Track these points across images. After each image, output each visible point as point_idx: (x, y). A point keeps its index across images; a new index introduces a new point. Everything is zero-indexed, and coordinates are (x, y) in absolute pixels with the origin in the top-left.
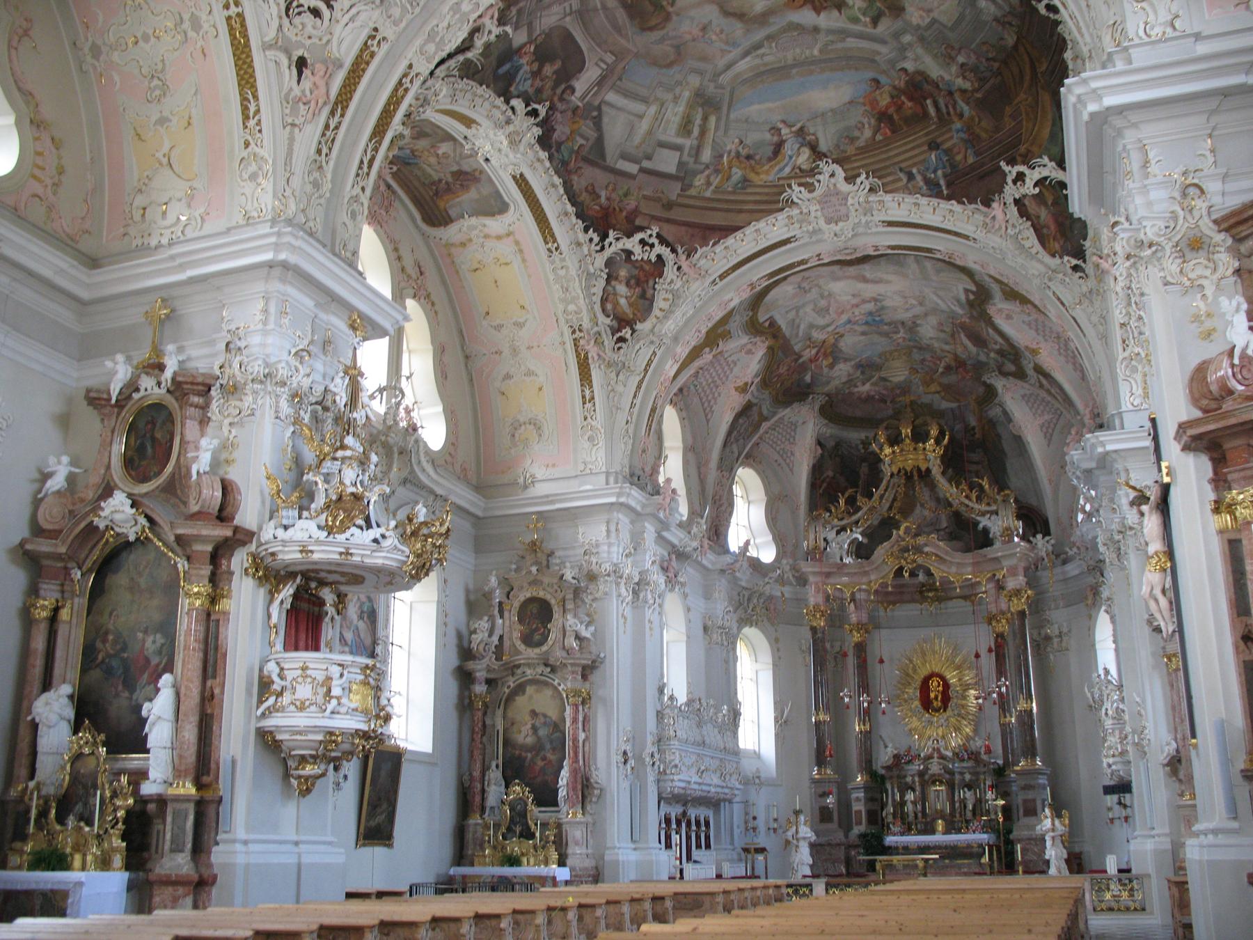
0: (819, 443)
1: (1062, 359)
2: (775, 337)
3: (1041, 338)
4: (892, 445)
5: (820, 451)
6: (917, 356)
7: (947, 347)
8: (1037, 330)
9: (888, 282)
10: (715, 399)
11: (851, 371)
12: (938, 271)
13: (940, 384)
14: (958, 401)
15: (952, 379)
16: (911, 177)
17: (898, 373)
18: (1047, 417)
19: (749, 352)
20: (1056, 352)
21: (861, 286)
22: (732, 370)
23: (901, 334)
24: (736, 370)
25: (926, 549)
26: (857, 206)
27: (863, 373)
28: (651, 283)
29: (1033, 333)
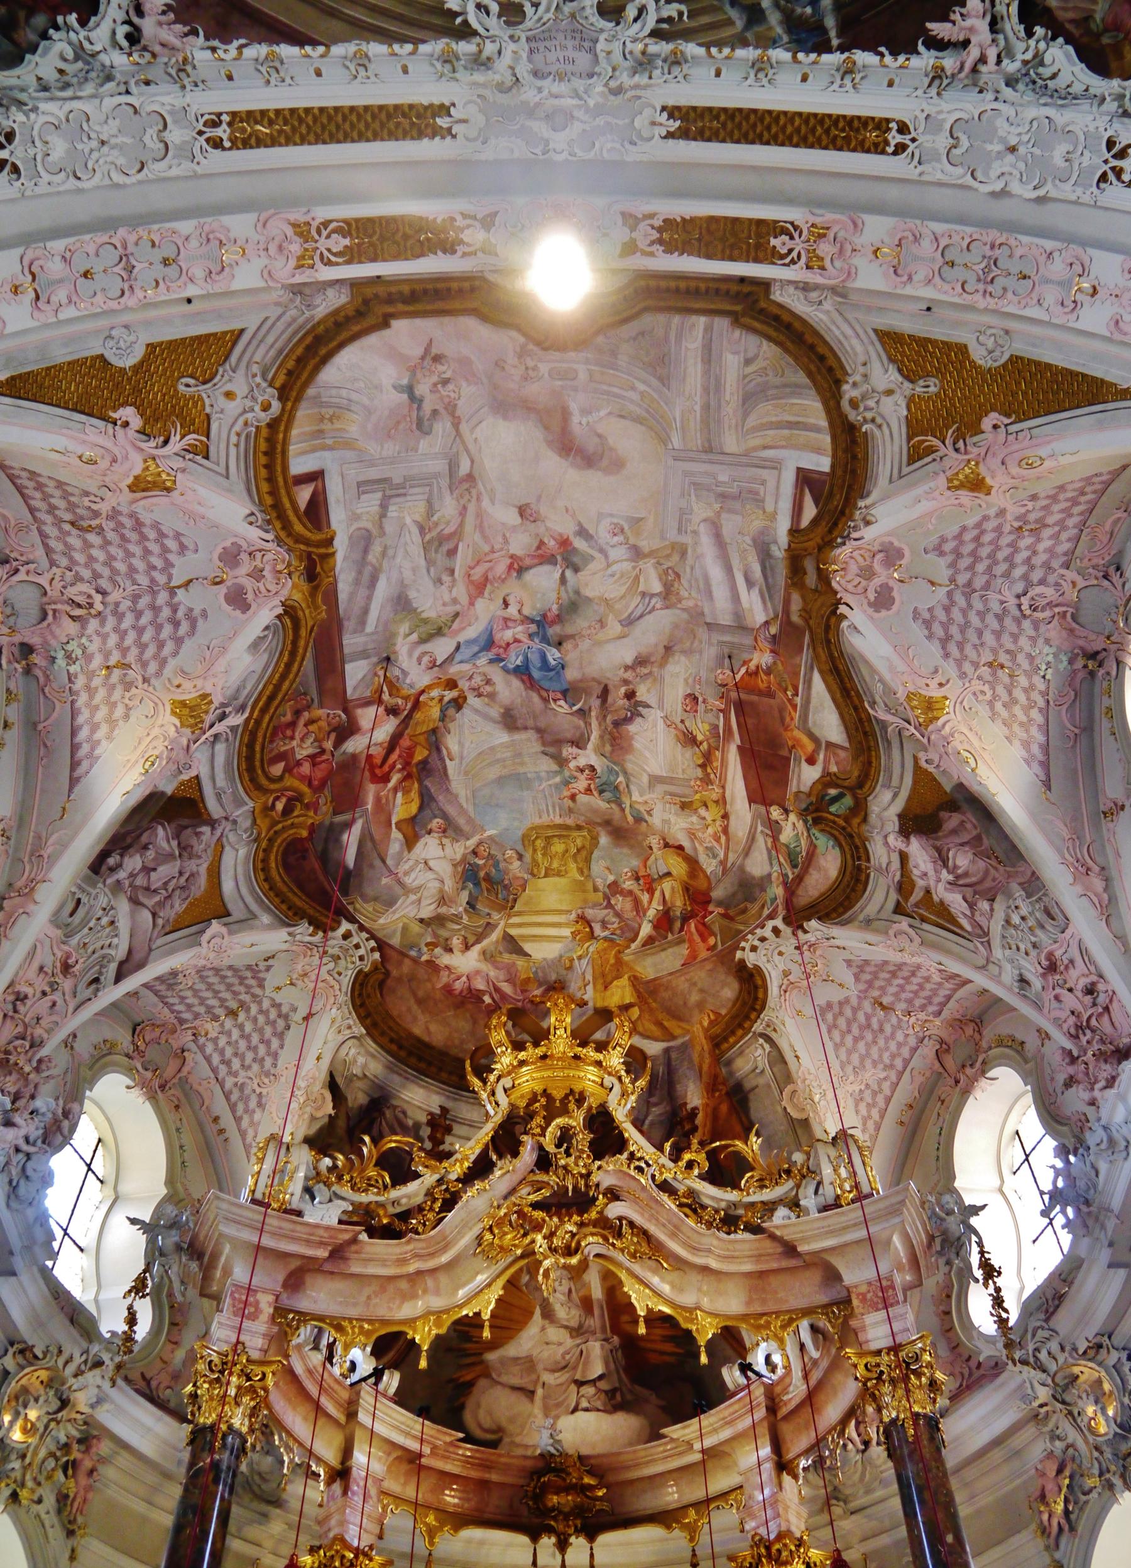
0: (333, 1085)
1: (998, 729)
2: (311, 575)
3: (950, 670)
4: (519, 1046)
5: (329, 1109)
6: (601, 872)
7: (679, 826)
8: (945, 641)
9: (618, 465)
10: (112, 723)
11: (449, 885)
12: (749, 399)
13: (635, 981)
14: (670, 1036)
15: (665, 963)
16: (755, 15)
17: (547, 932)
18: (871, 1075)
19: (238, 600)
20: (984, 711)
21: (552, 463)
22: (179, 641)
23: (588, 756)
24: (188, 644)
25: (615, 1210)
26: (617, 57)
27: (471, 905)
28: (40, 20)
29: (935, 648)
